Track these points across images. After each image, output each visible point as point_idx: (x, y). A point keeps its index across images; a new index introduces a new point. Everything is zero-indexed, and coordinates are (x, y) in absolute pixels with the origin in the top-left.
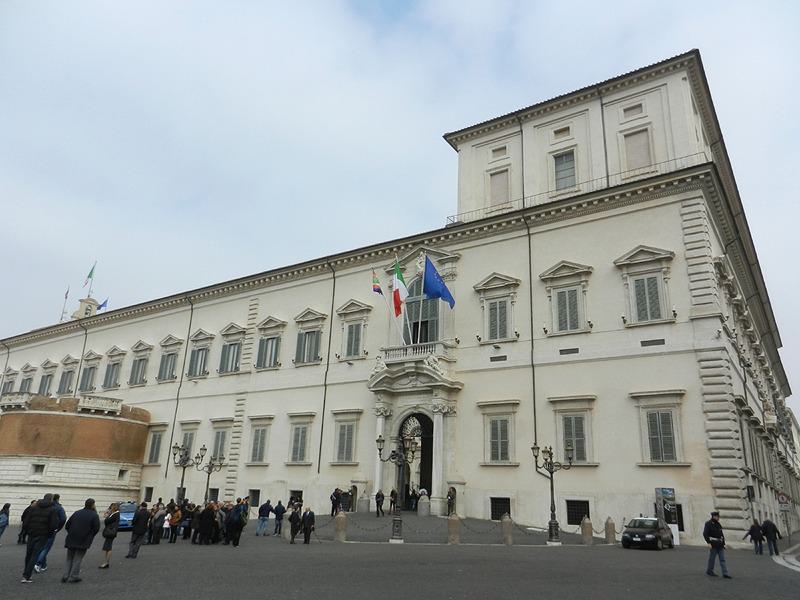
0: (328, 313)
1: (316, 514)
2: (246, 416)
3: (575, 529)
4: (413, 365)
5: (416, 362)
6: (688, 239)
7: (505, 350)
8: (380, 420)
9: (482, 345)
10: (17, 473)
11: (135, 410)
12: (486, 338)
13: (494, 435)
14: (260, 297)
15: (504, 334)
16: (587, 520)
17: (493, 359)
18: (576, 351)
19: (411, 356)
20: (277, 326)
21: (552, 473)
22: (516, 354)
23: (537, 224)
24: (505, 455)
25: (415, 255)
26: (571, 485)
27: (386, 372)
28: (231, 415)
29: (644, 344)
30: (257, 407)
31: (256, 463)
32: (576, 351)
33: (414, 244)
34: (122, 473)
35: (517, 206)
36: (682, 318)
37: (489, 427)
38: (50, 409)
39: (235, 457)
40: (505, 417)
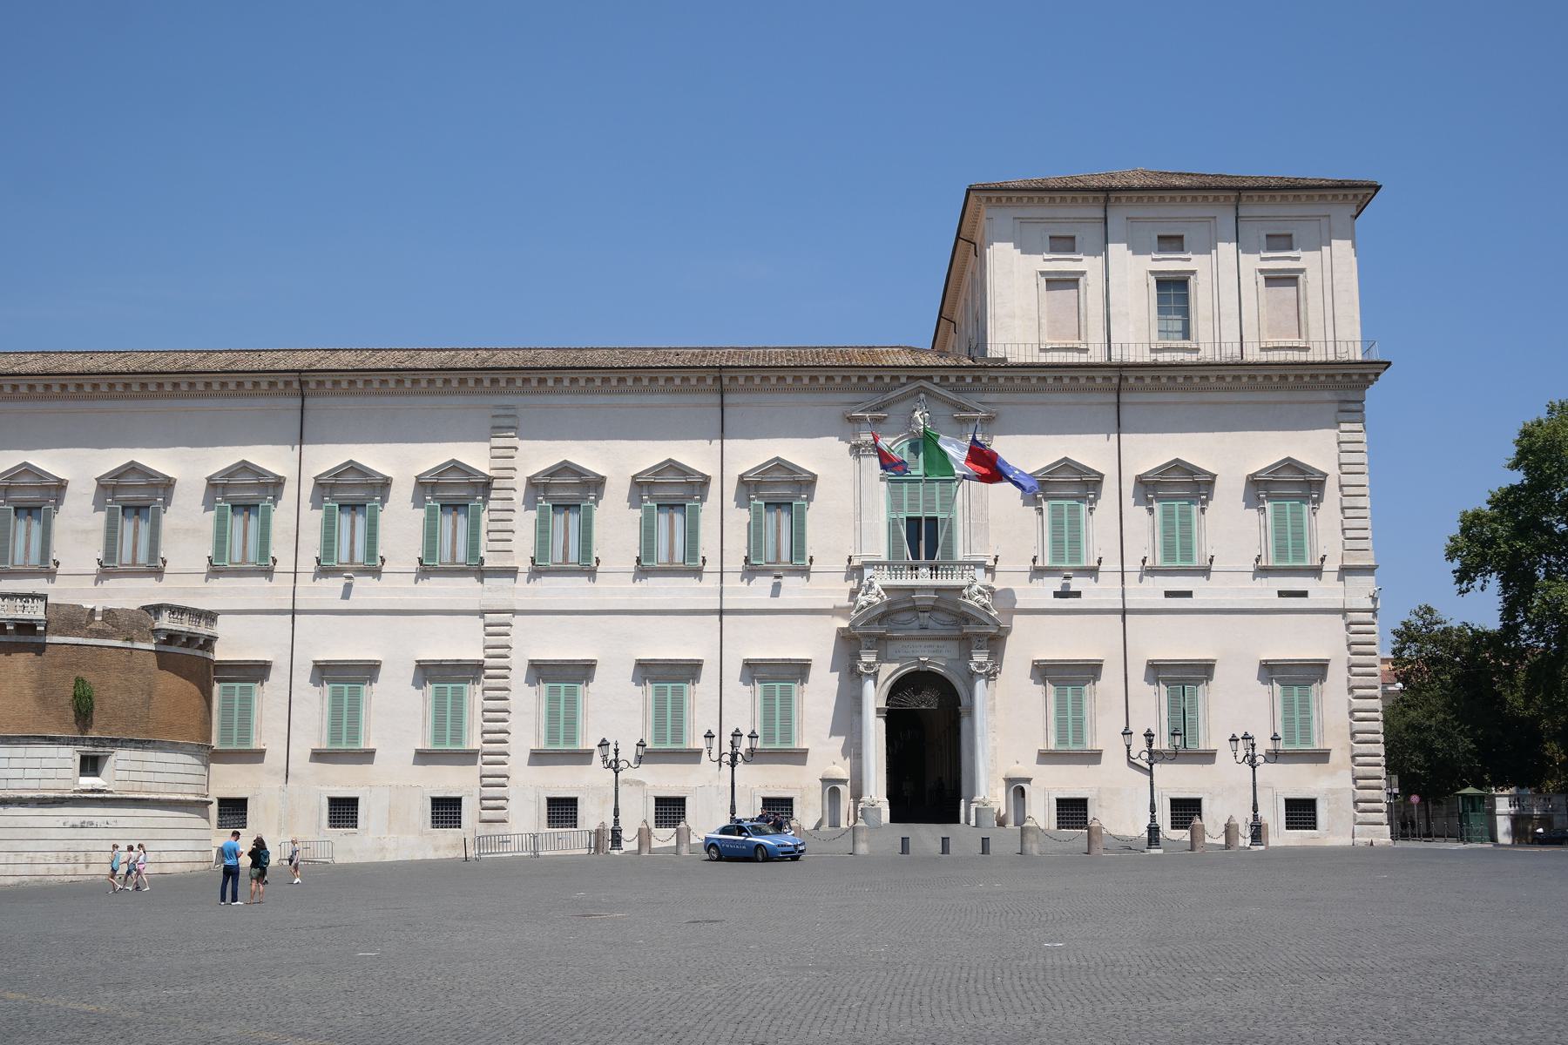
3: (1183, 835)
5: (938, 590)
6: (1346, 458)
7: (1076, 584)
10: (51, 773)
15: (1076, 556)
16: (1197, 821)
17: (1057, 595)
18: (1188, 594)
19: (924, 578)
21: (1151, 765)
23: (1132, 389)
26: (1177, 780)
28: (477, 655)
32: (1188, 594)
35: (1097, 355)
36: (1332, 565)
38: (100, 634)
39: (498, 735)
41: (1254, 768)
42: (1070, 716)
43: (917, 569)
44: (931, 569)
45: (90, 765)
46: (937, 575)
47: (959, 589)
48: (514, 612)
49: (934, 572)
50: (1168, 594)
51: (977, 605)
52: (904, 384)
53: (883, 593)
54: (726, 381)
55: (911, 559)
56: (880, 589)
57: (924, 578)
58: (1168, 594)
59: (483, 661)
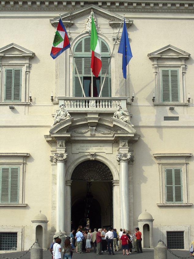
4: (97, 116)
5: (100, 114)
8: (60, 166)
9: (155, 105)
12: (159, 100)
13: (169, 181)
15: (176, 97)
17: (166, 118)
19: (92, 107)
24: (179, 198)
37: (164, 175)
40: (178, 167)
42: (174, 186)
43: (88, 103)
44: (96, 102)
46: (99, 105)
47: (111, 114)
49: (98, 104)
51: (122, 121)
52: (82, 6)
53: (68, 114)
55: (85, 96)
56: (67, 113)
57: (92, 107)
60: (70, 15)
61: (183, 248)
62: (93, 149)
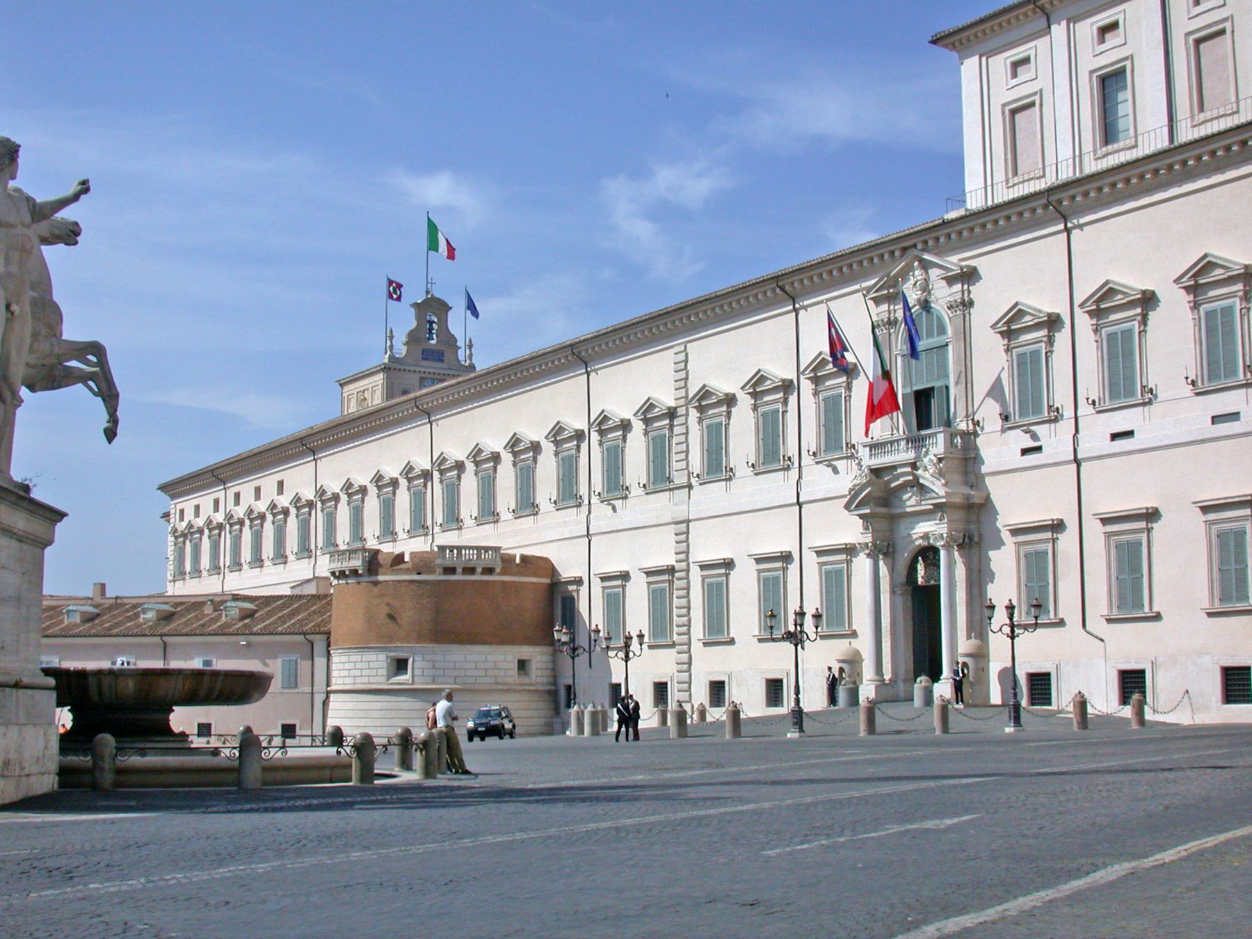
0: (792, 375)
1: (805, 710)
2: (691, 560)
11: (524, 558)
14: (689, 345)
17: (1025, 452)
18: (1129, 434)
20: (719, 403)
22: (1056, 441)
25: (908, 269)
27: (868, 484)
28: (669, 560)
29: (1215, 420)
30: (706, 548)
31: (714, 638)
32: (1129, 434)
33: (904, 250)
34: (522, 665)
41: (1013, 638)
45: (400, 665)
48: (688, 521)
50: (1115, 436)
54: (787, 288)
58: (1115, 436)
59: (673, 566)
60: (886, 279)
61: (1050, 704)
62: (923, 528)
